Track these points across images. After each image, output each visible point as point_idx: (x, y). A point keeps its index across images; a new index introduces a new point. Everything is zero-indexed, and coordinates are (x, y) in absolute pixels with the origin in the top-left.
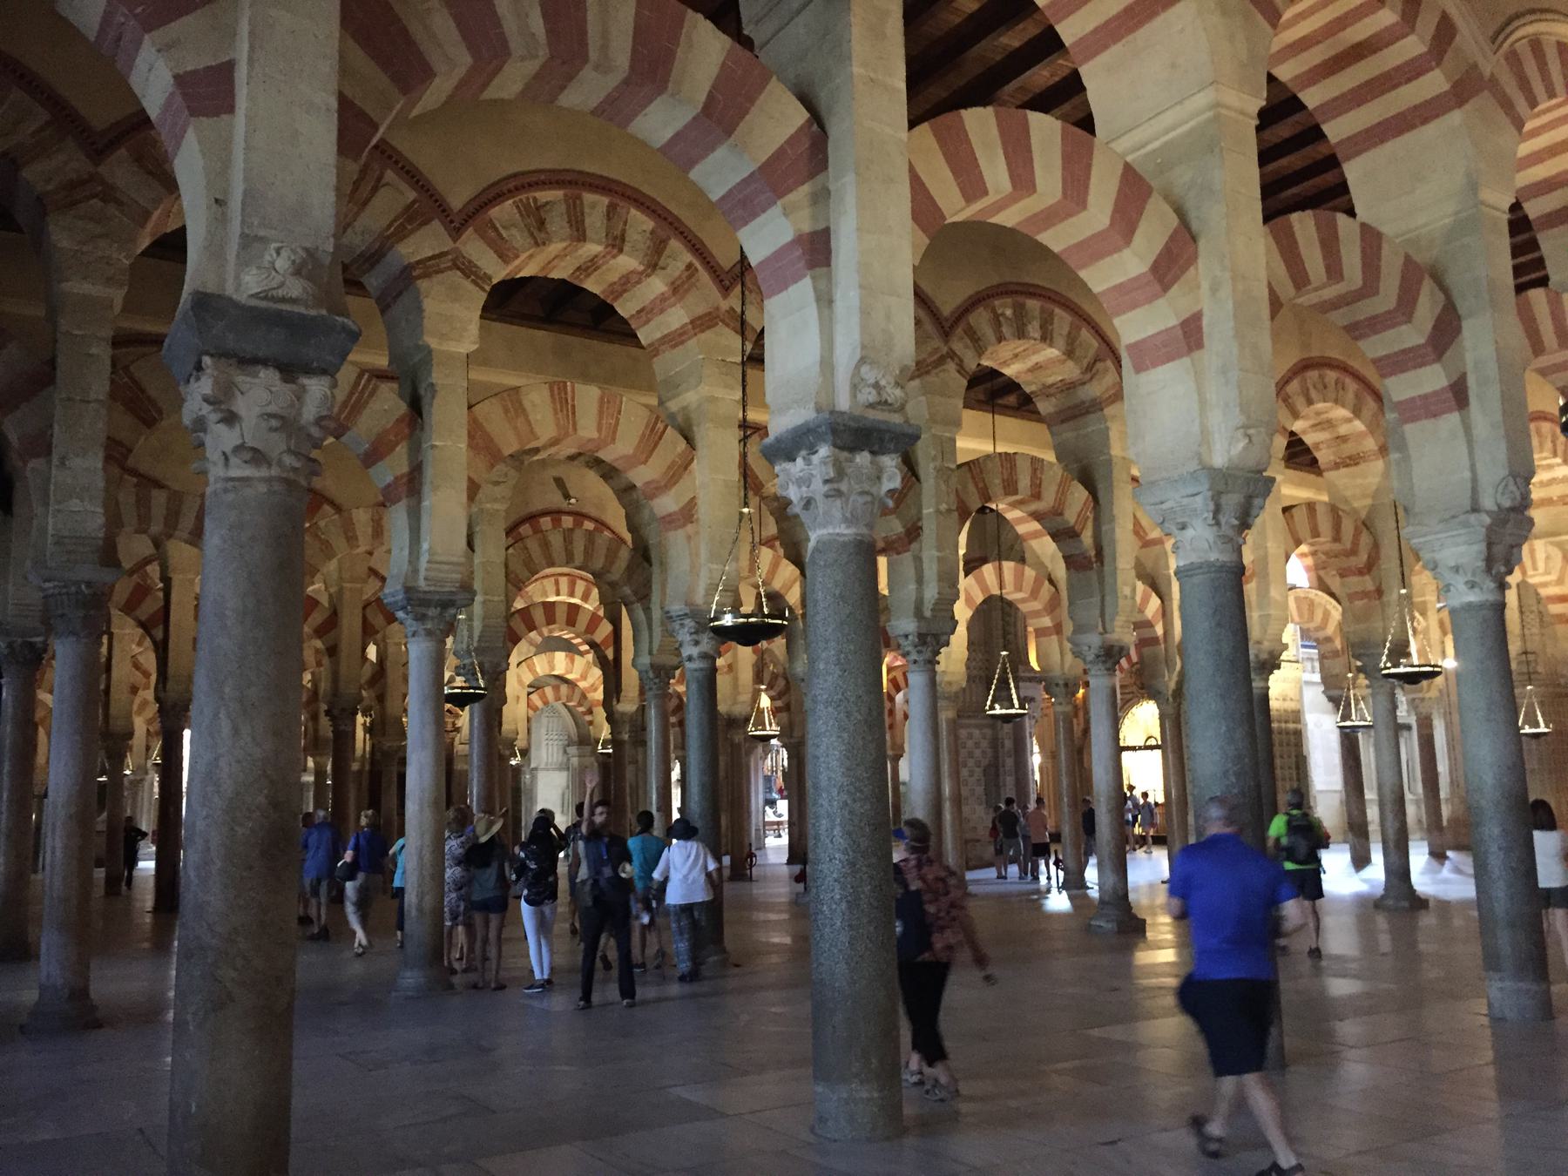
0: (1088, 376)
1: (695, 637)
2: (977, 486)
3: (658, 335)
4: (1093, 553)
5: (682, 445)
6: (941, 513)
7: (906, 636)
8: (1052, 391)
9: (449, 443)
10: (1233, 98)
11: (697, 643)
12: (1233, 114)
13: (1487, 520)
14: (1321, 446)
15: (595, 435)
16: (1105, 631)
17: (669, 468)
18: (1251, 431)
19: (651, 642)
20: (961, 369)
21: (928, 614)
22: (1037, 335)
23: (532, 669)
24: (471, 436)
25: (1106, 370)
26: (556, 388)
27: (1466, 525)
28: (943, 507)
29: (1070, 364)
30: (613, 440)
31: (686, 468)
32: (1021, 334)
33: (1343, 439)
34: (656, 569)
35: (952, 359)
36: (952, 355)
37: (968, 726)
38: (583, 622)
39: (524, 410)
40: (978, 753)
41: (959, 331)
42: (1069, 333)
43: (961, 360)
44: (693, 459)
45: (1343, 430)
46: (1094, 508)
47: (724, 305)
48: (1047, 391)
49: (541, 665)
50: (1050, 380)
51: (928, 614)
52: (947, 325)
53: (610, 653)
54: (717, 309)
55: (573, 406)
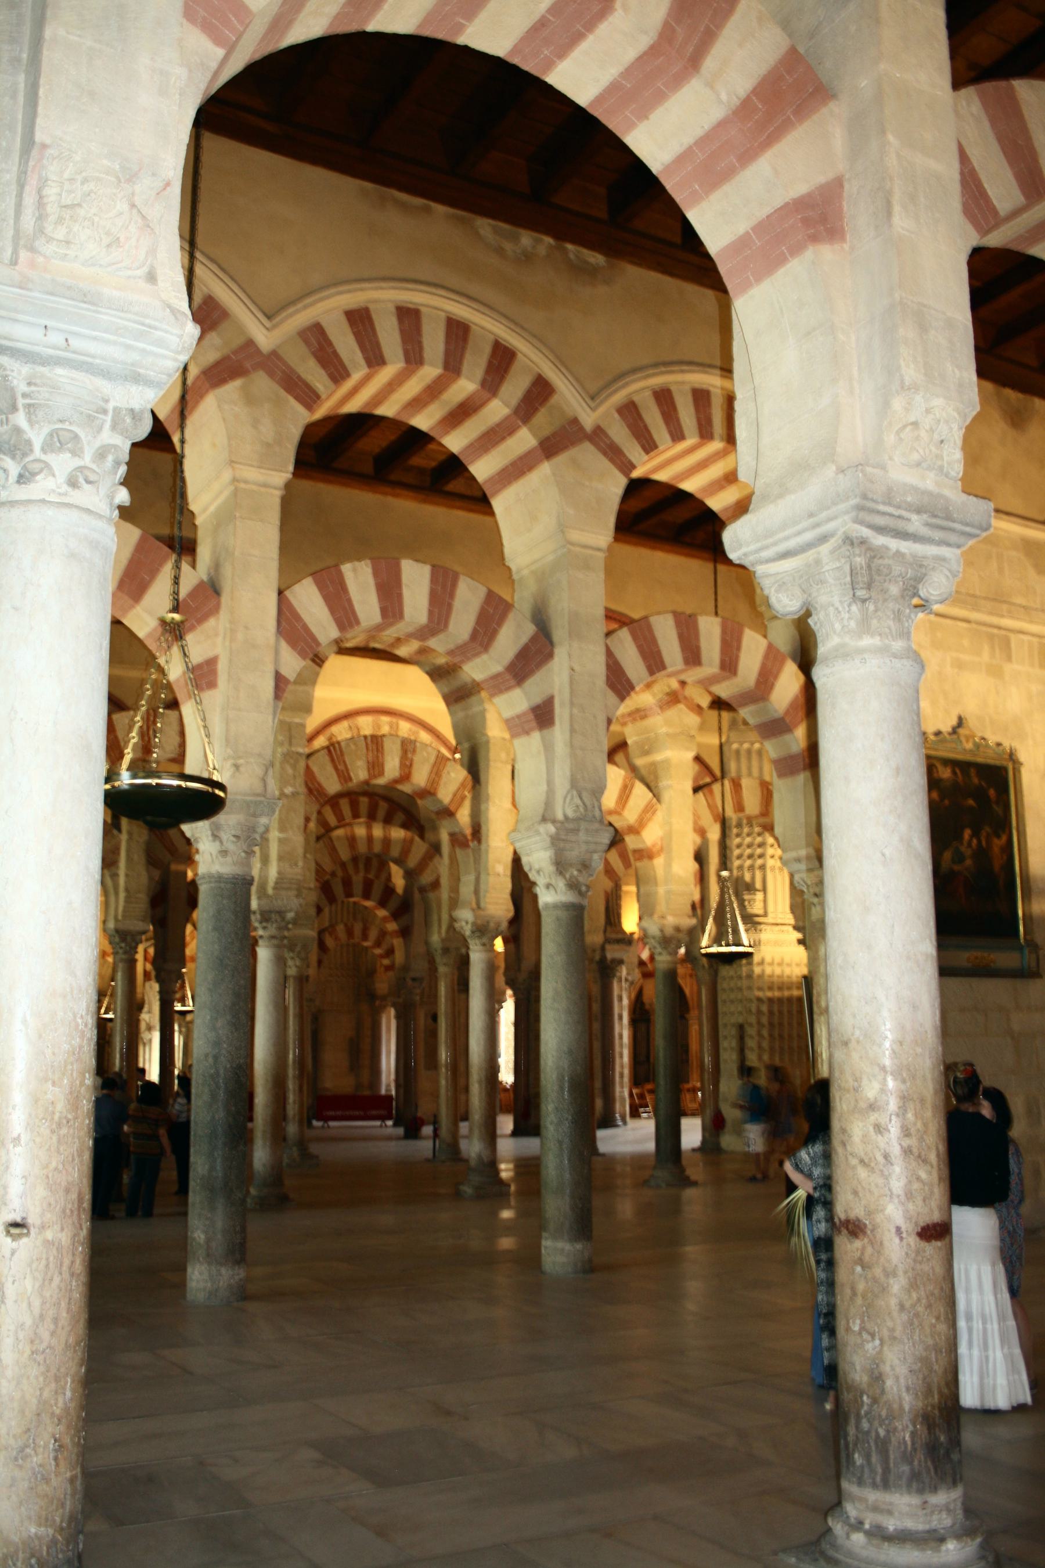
2: (336, 769)
4: (468, 831)
10: (252, 474)
12: (254, 487)
13: (551, 829)
16: (479, 907)
18: (241, 761)
21: (270, 891)
27: (538, 833)
28: (288, 790)
51: (270, 891)
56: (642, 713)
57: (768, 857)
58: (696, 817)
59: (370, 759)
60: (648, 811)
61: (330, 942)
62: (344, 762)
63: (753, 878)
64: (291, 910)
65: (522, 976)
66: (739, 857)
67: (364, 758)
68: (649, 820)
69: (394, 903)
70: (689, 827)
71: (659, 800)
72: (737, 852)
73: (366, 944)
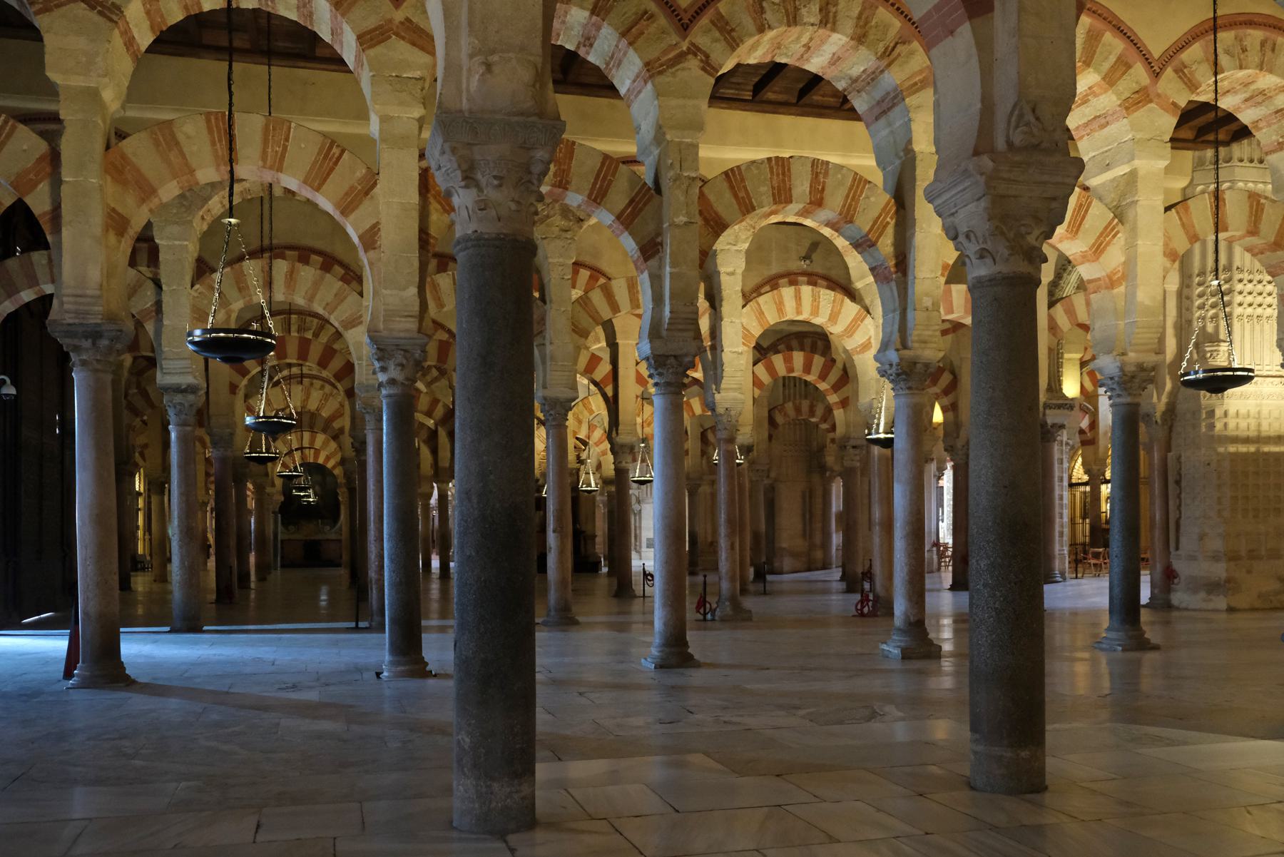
0: (885, 62)
2: (736, 196)
4: (892, 262)
6: (678, 226)
8: (859, 85)
14: (1261, 124)
17: (346, 194)
18: (495, 58)
20: (708, 66)
22: (815, 19)
25: (912, 53)
26: (213, 117)
29: (863, 51)
31: (367, 193)
32: (793, 19)
35: (696, 55)
36: (694, 50)
39: (177, 143)
42: (860, 14)
43: (707, 56)
44: (375, 184)
46: (897, 212)
47: (399, 16)
54: (390, 21)
56: (1103, 121)
57: (1235, 305)
58: (1168, 239)
59: (775, 184)
60: (1108, 233)
61: (780, 419)
62: (745, 187)
63: (1217, 328)
64: (686, 355)
65: (960, 443)
66: (1201, 307)
67: (768, 183)
68: (1108, 244)
69: (834, 376)
70: (1159, 248)
71: (1121, 221)
72: (1198, 302)
73: (813, 420)
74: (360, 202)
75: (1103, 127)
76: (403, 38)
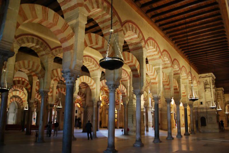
1: (70, 77)
3: (67, 7)
4: (139, 74)
5: (71, 31)
7: (110, 85)
9: (13, 9)
11: (70, 79)
15: (52, 22)
19: (44, 86)
21: (116, 80)
23: (12, 94)
24: (20, 11)
30: (56, 25)
33: (165, 64)
34: (46, 72)
36: (122, 30)
37: (90, 109)
38: (25, 84)
39: (35, 10)
40: (91, 113)
41: (124, 26)
44: (73, 35)
45: (166, 62)
48: (131, 44)
49: (14, 93)
50: (133, 42)
52: (123, 24)
53: (30, 91)
55: (48, 14)
74: (71, 38)
75: (154, 60)
76: (85, 7)
